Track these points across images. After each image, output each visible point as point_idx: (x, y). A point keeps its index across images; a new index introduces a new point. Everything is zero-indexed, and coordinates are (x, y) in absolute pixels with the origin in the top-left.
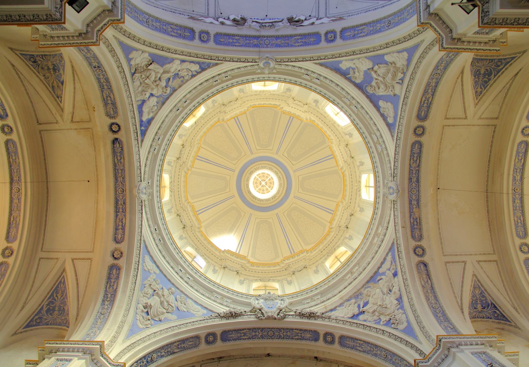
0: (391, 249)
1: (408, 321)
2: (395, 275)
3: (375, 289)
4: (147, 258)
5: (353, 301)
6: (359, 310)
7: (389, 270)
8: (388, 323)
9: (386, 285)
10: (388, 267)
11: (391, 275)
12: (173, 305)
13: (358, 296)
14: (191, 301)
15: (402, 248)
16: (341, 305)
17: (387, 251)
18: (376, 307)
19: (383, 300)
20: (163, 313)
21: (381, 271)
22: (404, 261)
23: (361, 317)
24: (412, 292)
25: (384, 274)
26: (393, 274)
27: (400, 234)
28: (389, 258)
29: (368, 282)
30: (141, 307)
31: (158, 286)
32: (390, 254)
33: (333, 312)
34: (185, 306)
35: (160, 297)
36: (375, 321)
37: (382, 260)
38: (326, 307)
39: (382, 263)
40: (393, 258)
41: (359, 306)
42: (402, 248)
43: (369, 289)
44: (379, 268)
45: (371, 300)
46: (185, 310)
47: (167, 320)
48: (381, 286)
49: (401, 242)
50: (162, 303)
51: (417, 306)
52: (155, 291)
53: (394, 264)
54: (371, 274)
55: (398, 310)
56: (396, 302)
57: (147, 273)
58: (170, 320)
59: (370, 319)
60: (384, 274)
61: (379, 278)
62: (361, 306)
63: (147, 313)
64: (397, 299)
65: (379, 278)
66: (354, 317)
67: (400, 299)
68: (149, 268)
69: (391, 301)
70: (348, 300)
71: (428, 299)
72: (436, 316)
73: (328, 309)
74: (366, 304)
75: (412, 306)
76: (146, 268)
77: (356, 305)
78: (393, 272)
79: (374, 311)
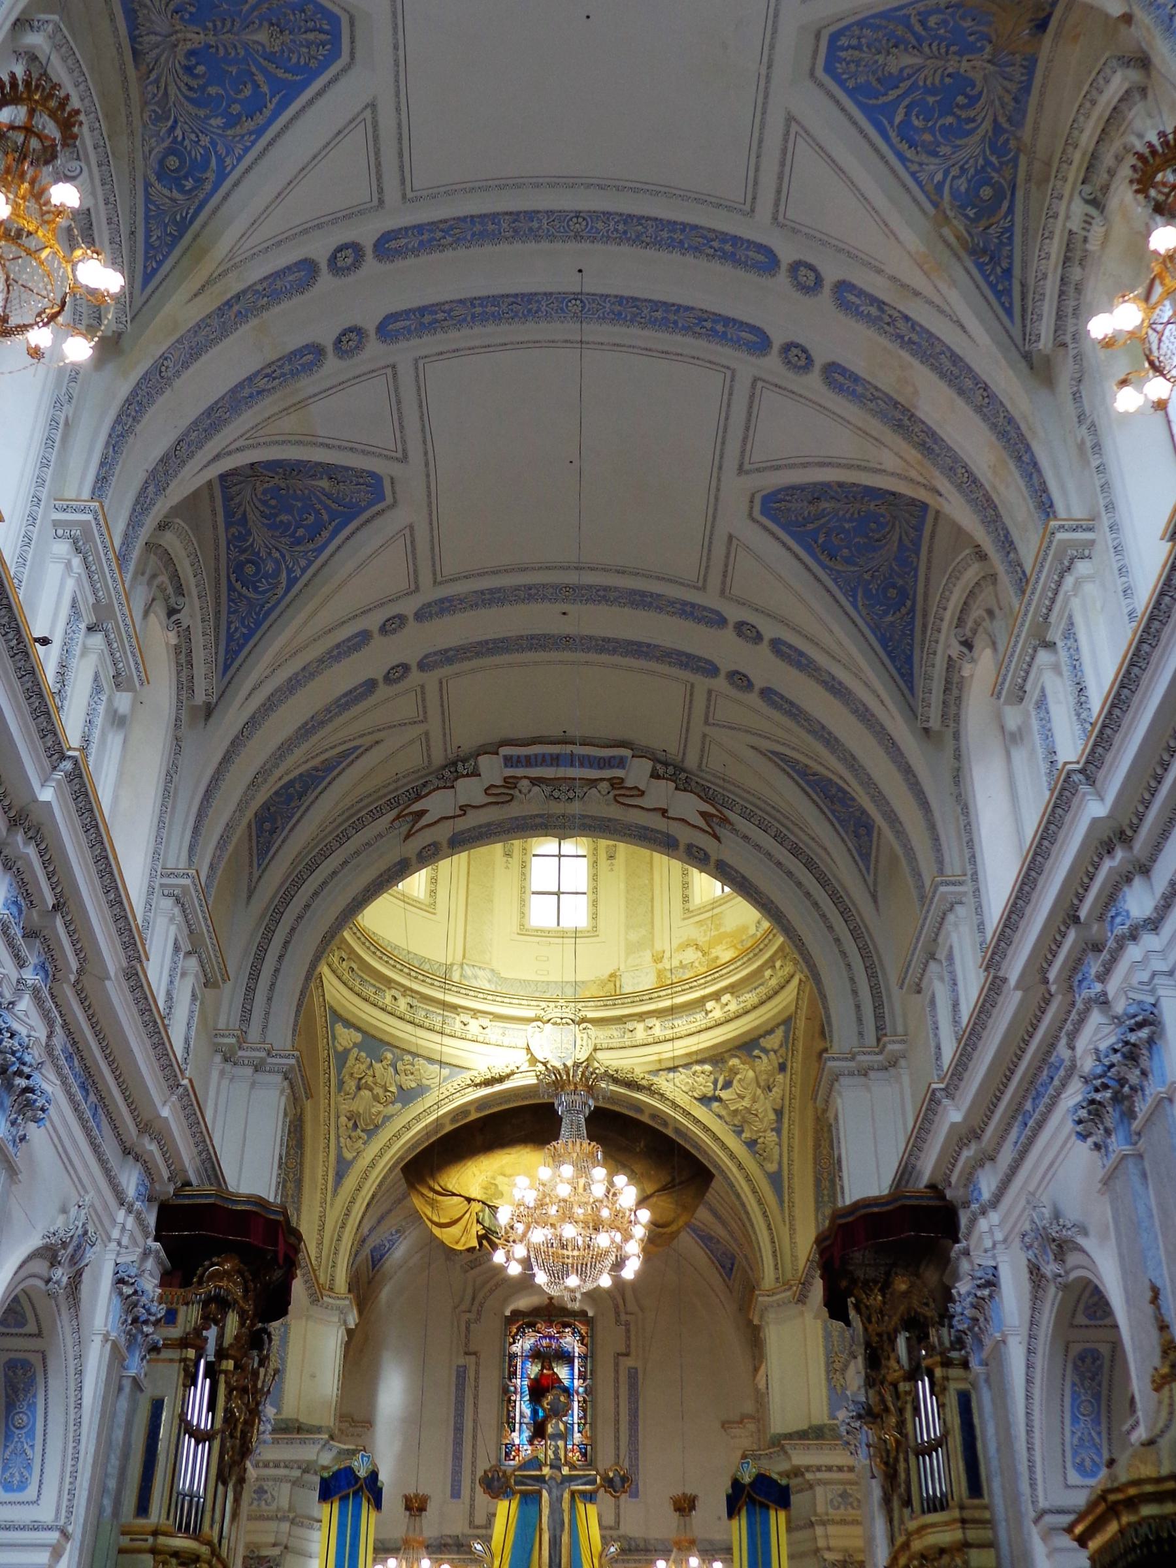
0: (787, 1022)
1: (780, 1164)
2: (782, 1068)
3: (747, 1067)
4: (339, 1028)
5: (708, 1067)
6: (715, 1089)
7: (775, 1052)
8: (751, 1144)
9: (764, 1077)
10: (776, 1047)
11: (776, 1065)
12: (394, 1089)
13: (717, 1062)
14: (422, 1061)
15: (800, 1046)
16: (686, 1066)
17: (779, 1020)
18: (739, 1106)
19: (754, 1100)
20: (379, 1113)
21: (764, 1042)
22: (798, 1066)
23: (715, 1105)
24: (797, 1124)
25: (765, 1051)
26: (780, 1064)
27: (801, 1024)
28: (780, 1032)
29: (739, 1048)
30: (343, 1119)
31: (363, 1067)
32: (782, 1028)
33: (671, 1075)
34: (411, 1077)
35: (371, 1090)
36: (735, 1125)
37: (769, 1027)
38: (660, 1061)
39: (770, 1032)
40: (786, 1037)
41: (715, 1083)
42: (800, 1046)
43: (734, 1062)
44: (761, 1036)
45: (735, 1083)
46: (413, 1085)
47: (387, 1118)
48: (757, 1069)
49: (800, 1033)
50: (376, 1098)
51: (796, 1155)
52: (360, 1079)
53: (784, 1049)
54: (747, 1039)
55: (772, 1130)
56: (772, 1116)
57: (343, 1057)
58: (392, 1116)
59: (728, 1119)
60: (765, 1051)
61: (756, 1052)
62: (719, 1086)
63: (355, 1126)
64: (775, 1110)
65: (756, 1052)
66: (705, 1100)
67: (779, 1113)
68: (344, 1043)
69: (765, 1108)
70: (701, 1062)
71: (817, 1146)
72: (818, 1182)
73: (664, 1066)
74: (728, 1085)
75: (791, 1148)
76: (340, 1049)
77: (712, 1077)
78: (781, 1060)
79: (736, 1111)
